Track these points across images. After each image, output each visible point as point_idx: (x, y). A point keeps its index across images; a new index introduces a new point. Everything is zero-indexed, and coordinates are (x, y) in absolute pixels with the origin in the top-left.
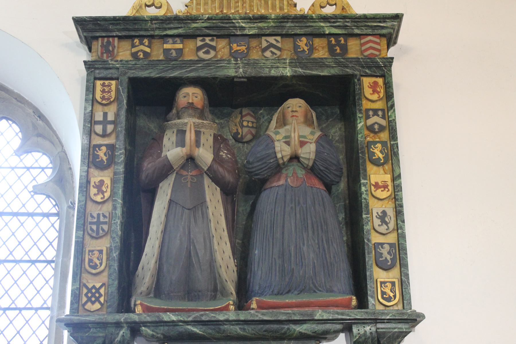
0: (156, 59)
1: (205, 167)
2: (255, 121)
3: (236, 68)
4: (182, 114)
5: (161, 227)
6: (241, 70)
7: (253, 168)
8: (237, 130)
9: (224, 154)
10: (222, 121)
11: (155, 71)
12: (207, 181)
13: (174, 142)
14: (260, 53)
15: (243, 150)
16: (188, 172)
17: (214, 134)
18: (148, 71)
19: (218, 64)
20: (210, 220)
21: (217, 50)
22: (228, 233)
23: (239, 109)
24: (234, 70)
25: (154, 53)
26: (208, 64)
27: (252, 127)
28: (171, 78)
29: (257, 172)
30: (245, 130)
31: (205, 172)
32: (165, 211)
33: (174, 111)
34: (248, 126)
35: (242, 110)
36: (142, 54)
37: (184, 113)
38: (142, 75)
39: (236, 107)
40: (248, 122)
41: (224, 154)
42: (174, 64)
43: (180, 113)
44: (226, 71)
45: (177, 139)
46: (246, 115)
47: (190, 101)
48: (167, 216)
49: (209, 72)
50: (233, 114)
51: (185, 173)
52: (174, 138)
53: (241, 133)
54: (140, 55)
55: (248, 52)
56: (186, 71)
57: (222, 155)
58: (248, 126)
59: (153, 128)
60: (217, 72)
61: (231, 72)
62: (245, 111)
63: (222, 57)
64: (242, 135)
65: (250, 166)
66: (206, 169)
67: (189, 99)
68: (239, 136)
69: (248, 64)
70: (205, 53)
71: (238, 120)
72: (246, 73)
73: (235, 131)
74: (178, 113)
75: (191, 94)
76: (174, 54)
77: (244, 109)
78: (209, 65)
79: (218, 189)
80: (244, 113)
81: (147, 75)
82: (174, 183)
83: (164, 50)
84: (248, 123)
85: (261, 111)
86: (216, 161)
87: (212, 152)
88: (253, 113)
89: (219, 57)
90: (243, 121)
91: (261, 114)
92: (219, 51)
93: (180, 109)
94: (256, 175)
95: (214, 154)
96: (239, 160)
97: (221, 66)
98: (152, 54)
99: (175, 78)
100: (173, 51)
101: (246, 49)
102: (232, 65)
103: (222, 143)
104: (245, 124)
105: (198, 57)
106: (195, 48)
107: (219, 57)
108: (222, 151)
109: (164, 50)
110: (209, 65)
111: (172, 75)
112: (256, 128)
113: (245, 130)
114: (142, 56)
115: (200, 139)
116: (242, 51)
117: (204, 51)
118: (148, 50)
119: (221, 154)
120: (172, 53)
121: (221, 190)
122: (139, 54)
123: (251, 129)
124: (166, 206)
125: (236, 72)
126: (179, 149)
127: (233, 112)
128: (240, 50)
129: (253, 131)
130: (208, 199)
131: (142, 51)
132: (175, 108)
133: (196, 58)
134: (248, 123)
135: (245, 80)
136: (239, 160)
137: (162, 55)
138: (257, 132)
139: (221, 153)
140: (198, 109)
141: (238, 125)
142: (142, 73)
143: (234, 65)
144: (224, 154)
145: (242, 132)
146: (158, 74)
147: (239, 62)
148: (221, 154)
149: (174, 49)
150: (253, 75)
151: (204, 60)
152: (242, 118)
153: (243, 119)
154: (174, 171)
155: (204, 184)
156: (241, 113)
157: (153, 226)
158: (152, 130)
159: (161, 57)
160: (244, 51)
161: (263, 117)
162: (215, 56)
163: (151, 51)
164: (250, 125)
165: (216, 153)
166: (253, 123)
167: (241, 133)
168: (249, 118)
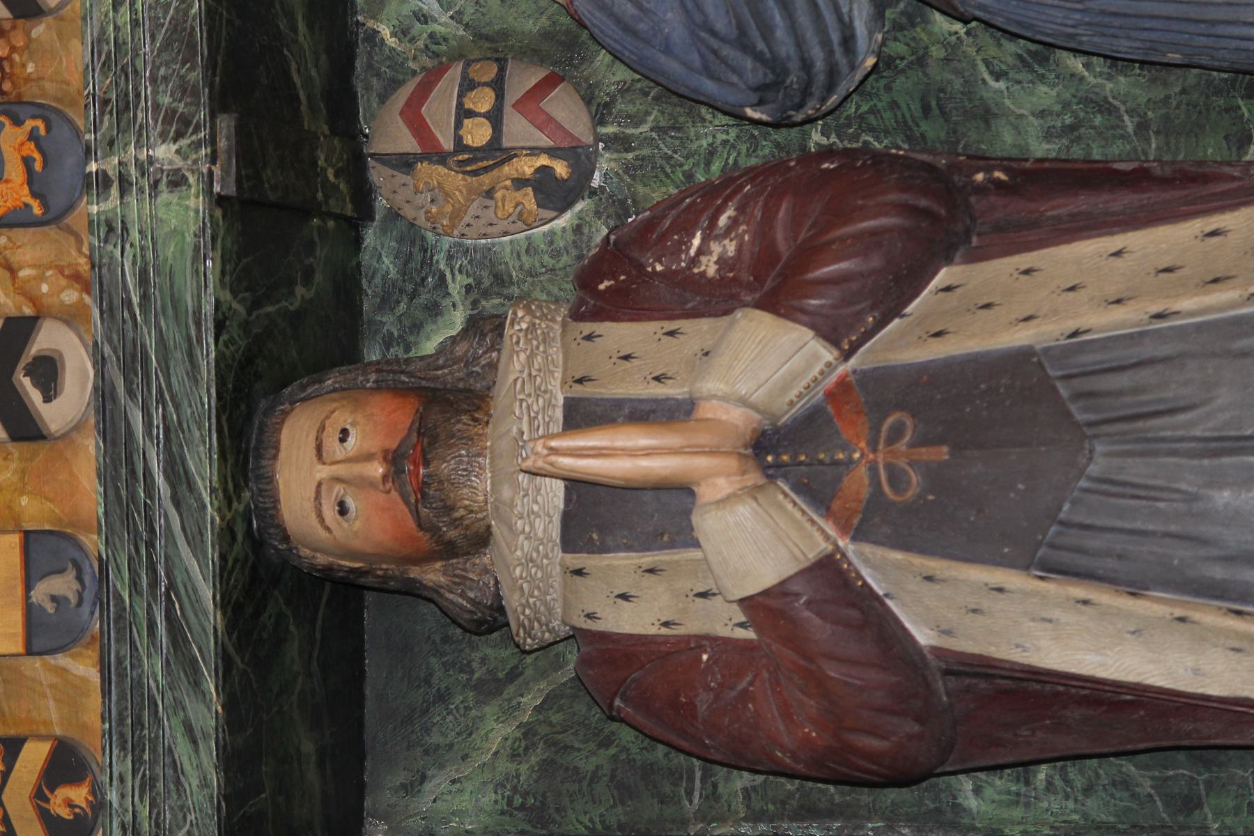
0: (95, 702)
1: (816, 357)
2: (456, 71)
3: (155, 185)
4: (456, 523)
5: (1210, 616)
6: (164, 152)
7: (806, 65)
8: (520, 183)
9: (716, 248)
10: (456, 287)
11: (178, 705)
12: (901, 345)
13: (648, 559)
14: (39, 30)
15: (649, 141)
16: (850, 461)
17: (577, 315)
18: (183, 749)
19: (128, 303)
20: (1159, 316)
21: (28, 311)
22: (1234, 207)
23: (378, 175)
24: (165, 196)
25: (53, 716)
26: (124, 363)
27: (498, 85)
28: (226, 603)
29: (835, 37)
30: (518, 129)
31: (847, 356)
32: (1104, 597)
33: (432, 575)
34: (495, 117)
35: (383, 159)
36: (64, 792)
37: (449, 509)
38: (204, 784)
39: (363, 195)
40: (464, 113)
41: (712, 252)
42: (134, 585)
43: (452, 534)
44: (170, 251)
45: (629, 548)
46: (419, 128)
47: (377, 470)
48: (1136, 588)
49: (178, 355)
50: (408, 212)
51: (857, 483)
52: (622, 564)
53: (543, 160)
54: (70, 804)
55: (42, 112)
56: (177, 503)
57: (721, 261)
58: (495, 117)
59: (509, 729)
60: (176, 302)
61: (183, 215)
62: (389, 134)
63: (76, 277)
64: (552, 152)
65: (794, 78)
66: (827, 354)
67: (362, 483)
68: (561, 169)
69: (125, 106)
70: (50, 389)
71: (455, 181)
72: (185, 122)
73: (528, 198)
74: (448, 550)
75: (323, 472)
76: (63, 585)
77: (380, 145)
78: (133, 361)
79: (943, 276)
80: (407, 143)
81: (209, 756)
82: (924, 551)
83: (29, 652)
84: (471, 114)
85: (385, 32)
86: (774, 292)
87: (705, 324)
88: (395, 84)
89: (71, 296)
90: (460, 146)
91: (402, 32)
92: (33, 300)
93: (424, 537)
94: (848, 41)
95: (727, 312)
96: (716, 167)
97: (143, 280)
98: (58, 731)
99: (223, 573)
100: (40, 593)
101: (18, 122)
102: (136, 209)
103: (641, 267)
104: (478, 134)
105: (78, 427)
106: (15, 449)
107: (71, 296)
108: (694, 261)
109: (29, 652)
110: (133, 361)
111: (207, 593)
112: (502, 63)
113: (518, 129)
114: (80, 794)
115: (618, 404)
116: (30, 149)
117: (35, 396)
118: (34, 756)
119: (712, 271)
120: (54, 599)
121: (949, 261)
122: (65, 813)
123: (512, 96)
124: (1078, 591)
125: (177, 181)
126: (707, 523)
127: (394, 215)
128: (27, 162)
129: (523, 79)
130: (1021, 337)
131: (39, 796)
132: (414, 572)
133: (90, 446)
134: (471, 114)
135: (226, 124)
136: (716, 167)
137: (61, 660)
138: (532, 52)
139: (709, 266)
140: (421, 418)
141: (486, 179)
142: (192, 781)
143: (132, 199)
144: (712, 252)
145: (535, 151)
146: (196, 684)
147: (111, 165)
148: (712, 271)
149: (28, 588)
150: (196, 76)
151: (103, 396)
152: (441, 158)
153: (447, 144)
154: (844, 555)
155: (923, 368)
156: (405, 163)
157: (1196, 671)
158: (528, 731)
159: (83, 667)
160: (33, 136)
161: (423, 18)
162: (72, 317)
163: (41, 738)
164: (483, 101)
165: (716, 298)
166: (468, 85)
167: (543, 160)
168: (439, 111)
